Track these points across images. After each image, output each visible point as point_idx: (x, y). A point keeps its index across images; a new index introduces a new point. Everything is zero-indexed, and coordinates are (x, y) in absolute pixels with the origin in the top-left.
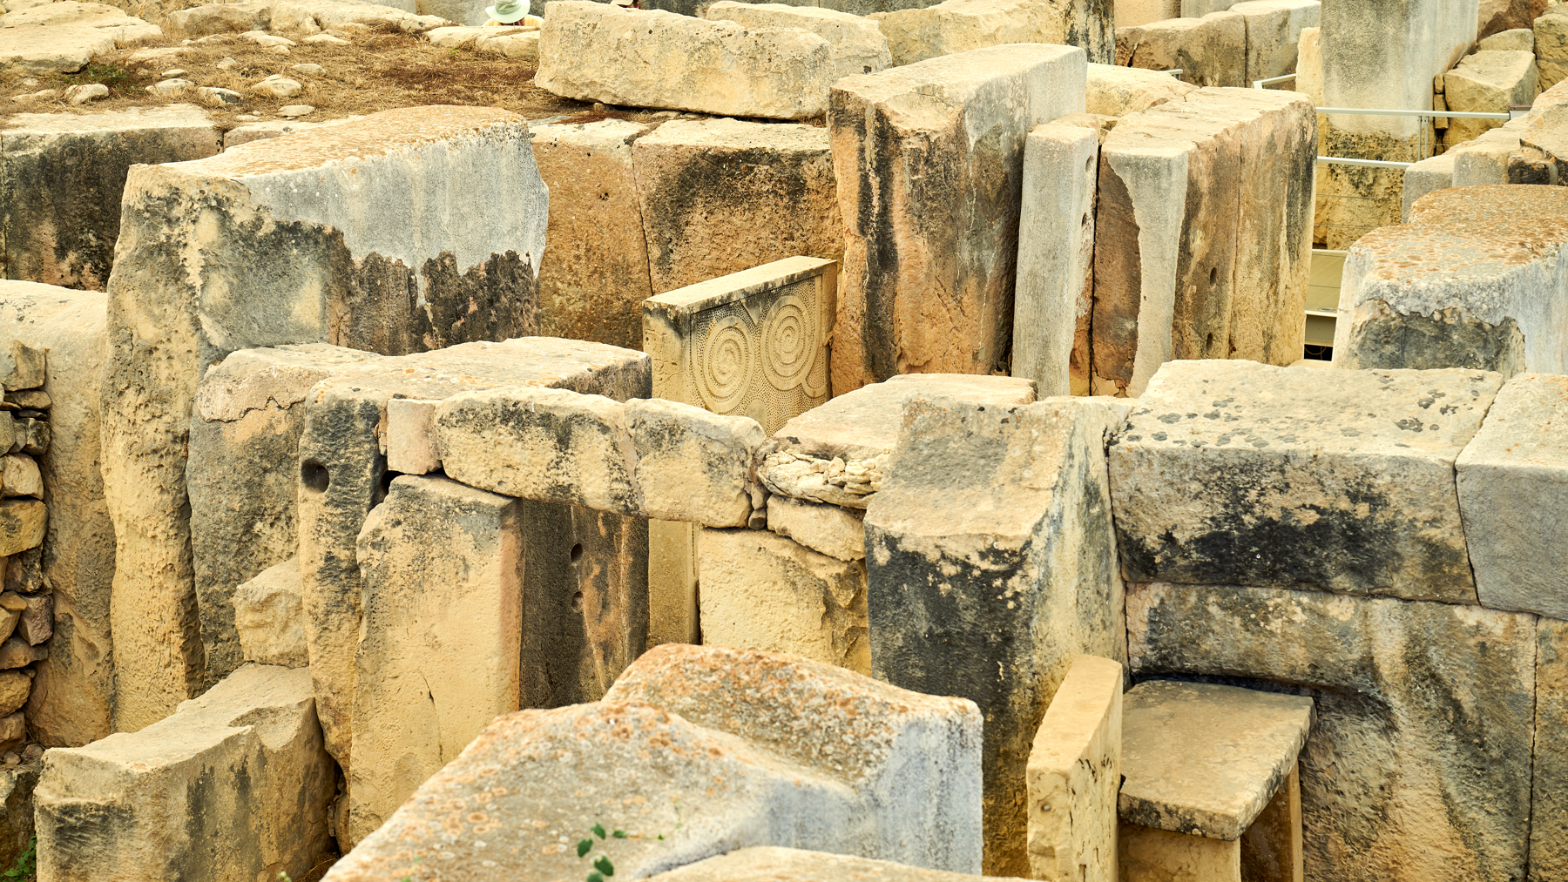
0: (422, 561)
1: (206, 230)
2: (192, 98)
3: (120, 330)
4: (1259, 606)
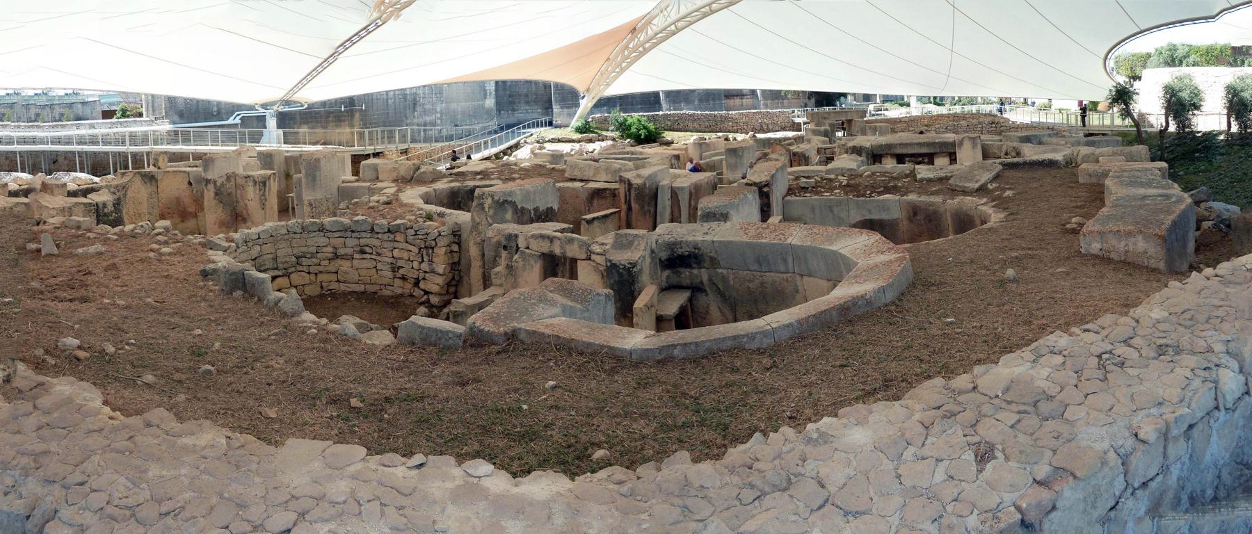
1: (489, 201)
3: (473, 219)
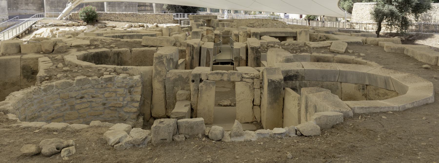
1: (165, 59)
2: (104, 47)
3: (156, 70)
4: (288, 83)
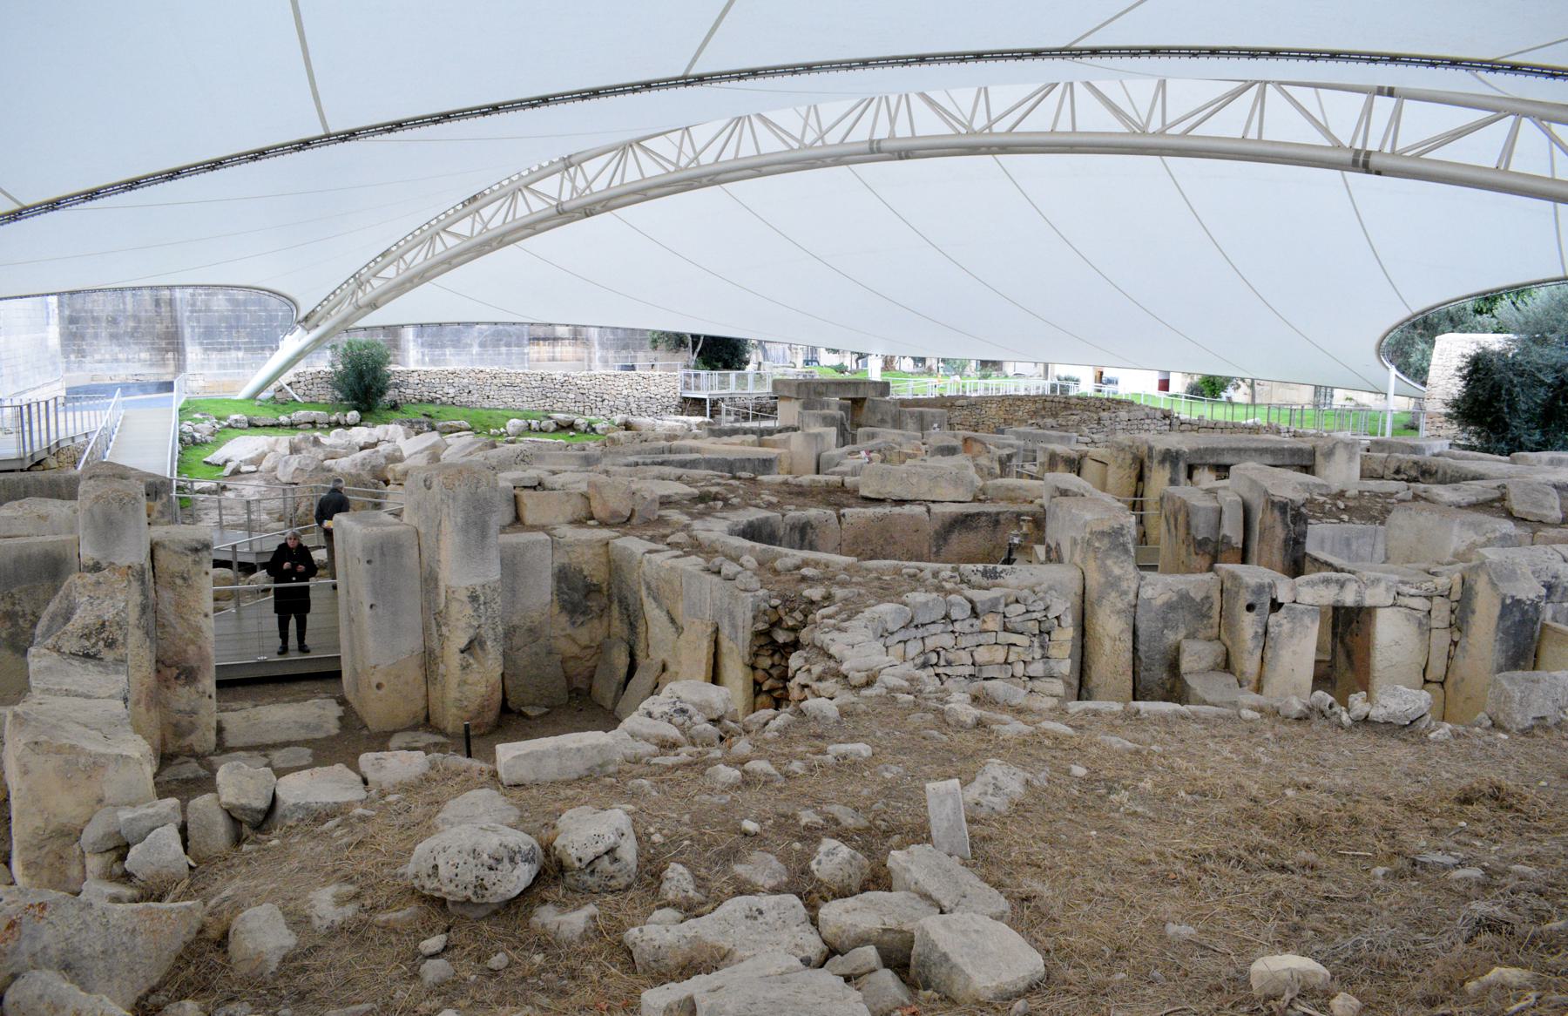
0: (1293, 630)
